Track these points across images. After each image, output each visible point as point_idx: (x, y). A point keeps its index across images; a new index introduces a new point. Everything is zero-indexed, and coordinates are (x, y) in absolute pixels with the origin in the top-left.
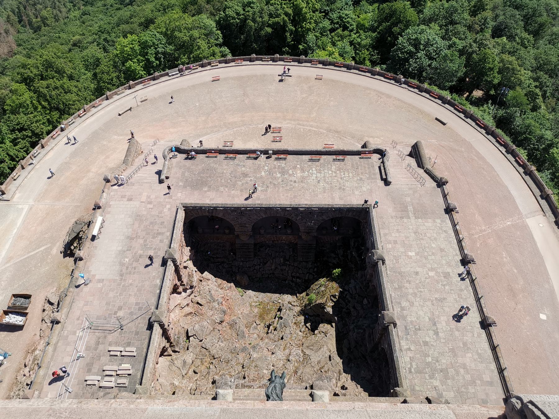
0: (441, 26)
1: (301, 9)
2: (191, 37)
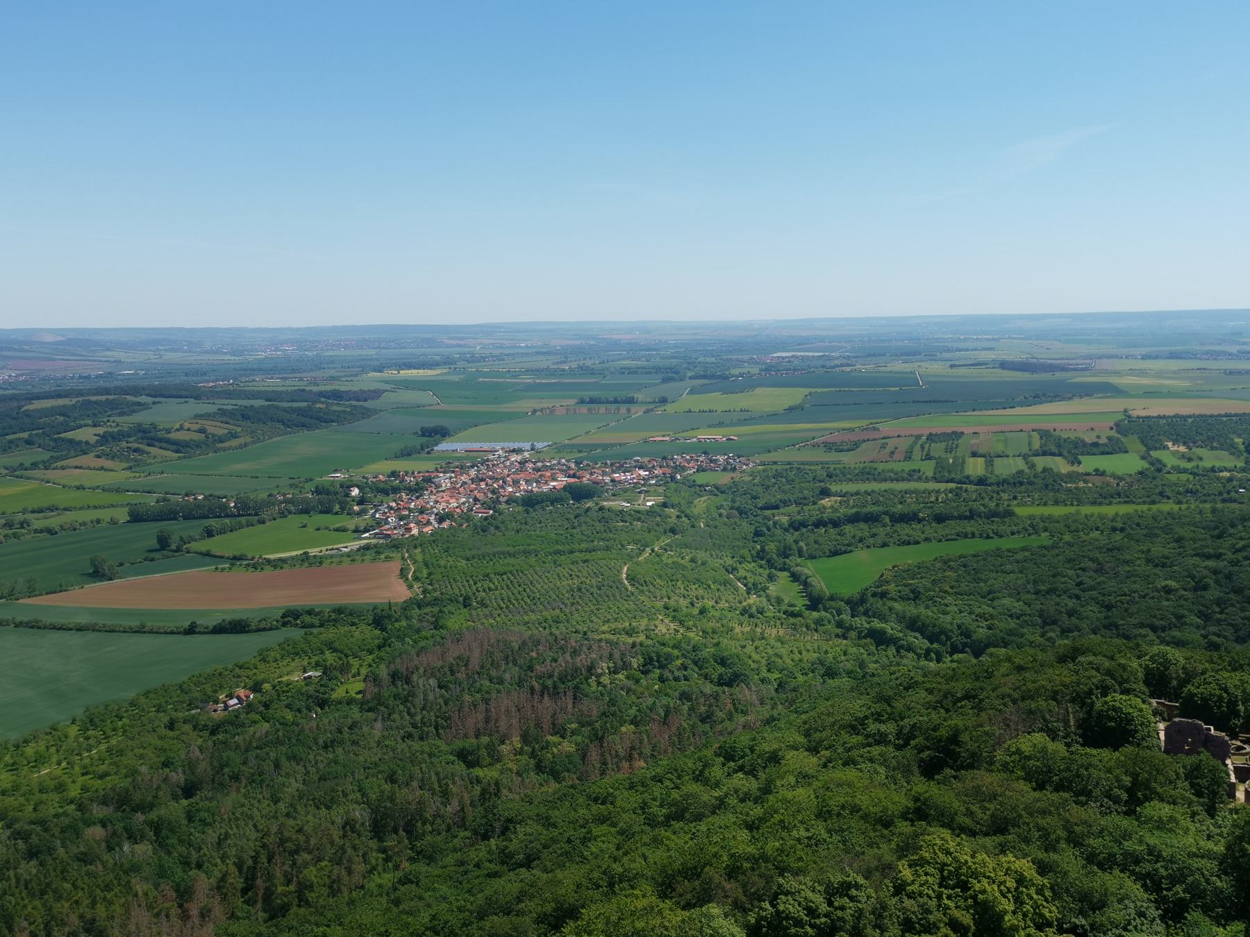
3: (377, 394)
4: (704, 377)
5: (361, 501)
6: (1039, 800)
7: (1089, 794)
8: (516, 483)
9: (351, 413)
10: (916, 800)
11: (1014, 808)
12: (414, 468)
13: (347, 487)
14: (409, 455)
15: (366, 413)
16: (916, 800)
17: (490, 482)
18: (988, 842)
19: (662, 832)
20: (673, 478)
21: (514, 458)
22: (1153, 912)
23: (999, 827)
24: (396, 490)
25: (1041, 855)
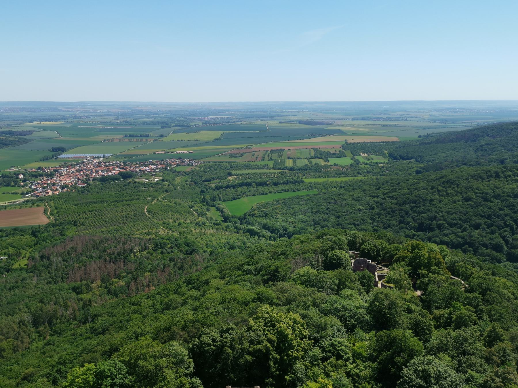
0: (452, 357)
1: (287, 336)
2: (156, 366)
3: (30, 132)
4: (179, 126)
5: (24, 181)
6: (304, 291)
7: (323, 288)
8: (97, 172)
9: (18, 141)
10: (258, 294)
11: (294, 295)
12: (49, 166)
13: (17, 174)
14: (47, 160)
15: (26, 141)
16: (258, 294)
17: (85, 171)
18: (284, 308)
19: (159, 315)
20: (166, 169)
21: (96, 161)
22: (343, 330)
23: (288, 302)
24: (41, 175)
25: (303, 312)
